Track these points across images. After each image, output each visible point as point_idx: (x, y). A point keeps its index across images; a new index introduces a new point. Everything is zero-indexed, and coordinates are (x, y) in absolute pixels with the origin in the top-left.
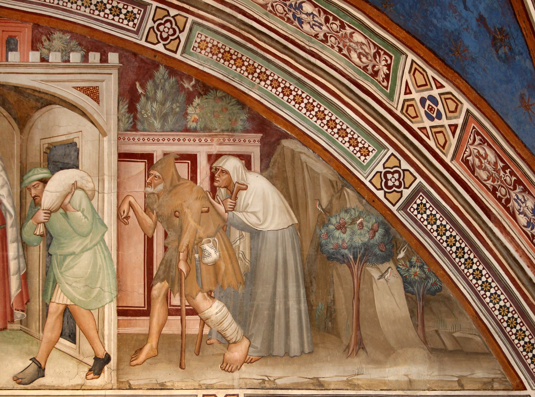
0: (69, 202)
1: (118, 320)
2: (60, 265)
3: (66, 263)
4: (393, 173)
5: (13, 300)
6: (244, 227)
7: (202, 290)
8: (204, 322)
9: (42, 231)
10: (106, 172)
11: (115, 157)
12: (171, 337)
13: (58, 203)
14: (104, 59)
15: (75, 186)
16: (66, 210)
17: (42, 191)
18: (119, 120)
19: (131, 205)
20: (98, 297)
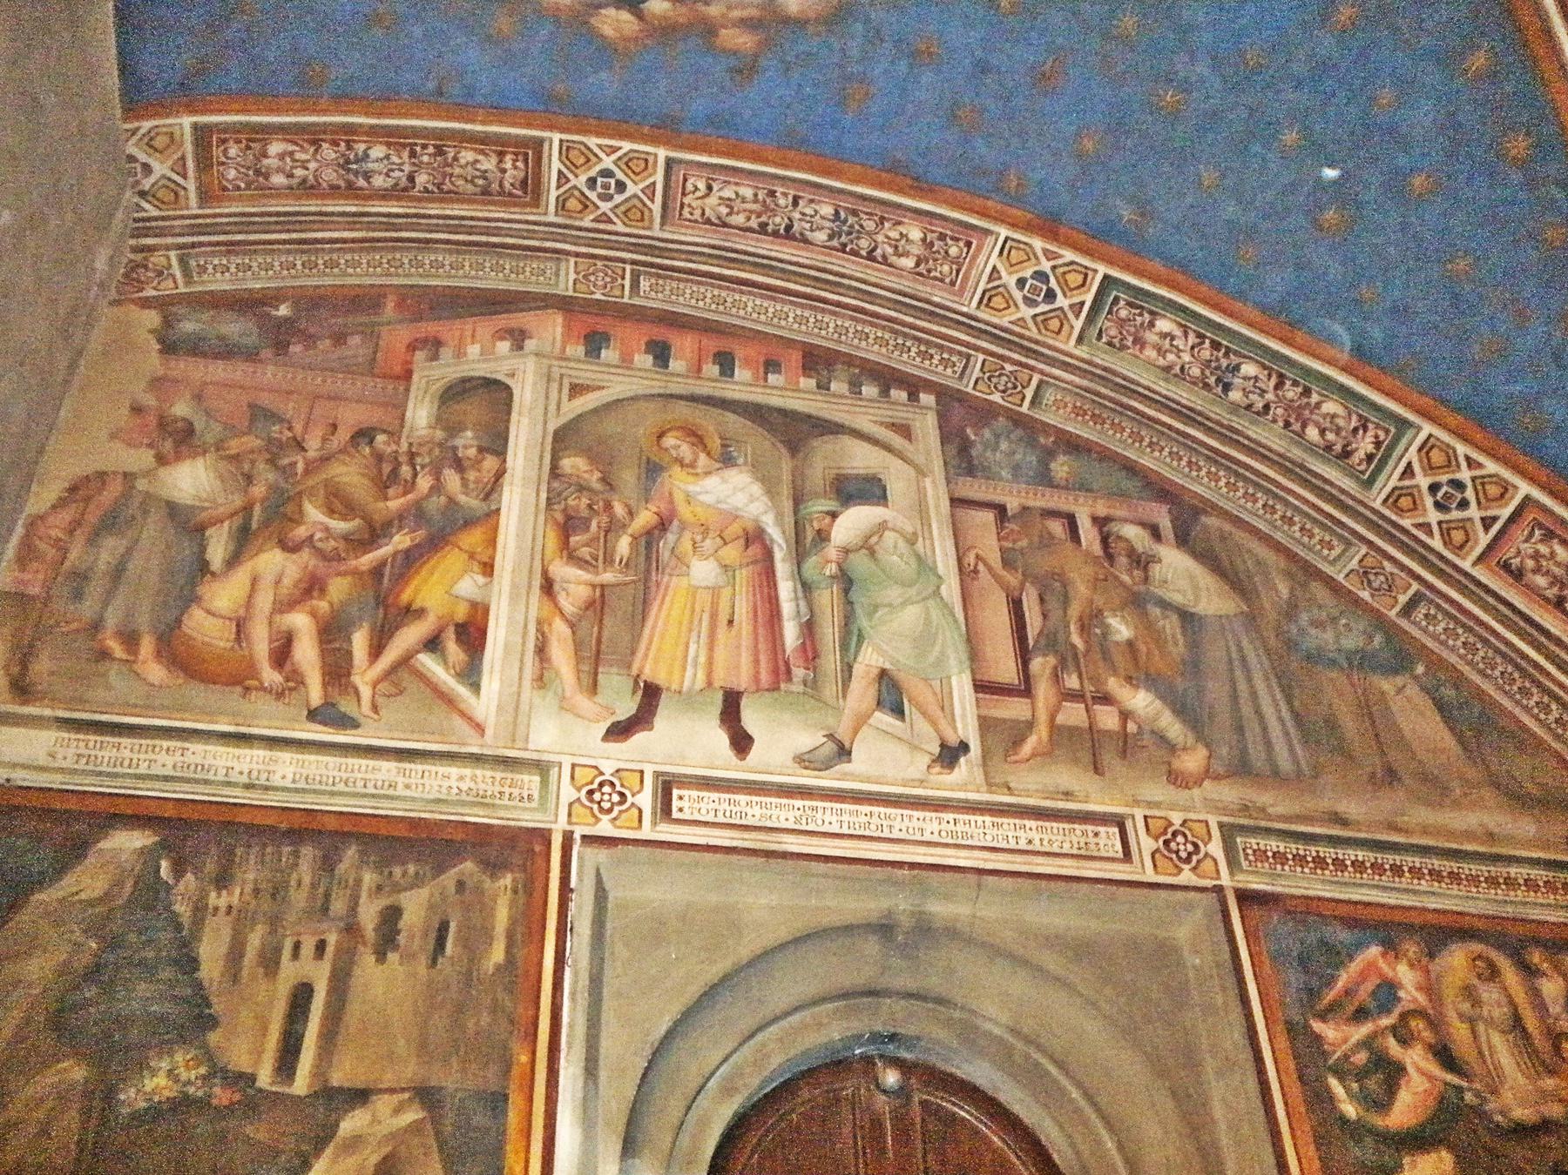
0: (877, 543)
1: (977, 699)
2: (870, 615)
3: (878, 615)
4: (1376, 574)
5: (788, 651)
6: (1165, 605)
7: (1115, 673)
8: (1125, 715)
9: (834, 570)
10: (933, 515)
11: (945, 504)
12: (1073, 731)
13: (858, 541)
14: (913, 396)
15: (882, 527)
16: (872, 553)
17: (831, 525)
18: (946, 463)
19: (978, 557)
20: (940, 662)
